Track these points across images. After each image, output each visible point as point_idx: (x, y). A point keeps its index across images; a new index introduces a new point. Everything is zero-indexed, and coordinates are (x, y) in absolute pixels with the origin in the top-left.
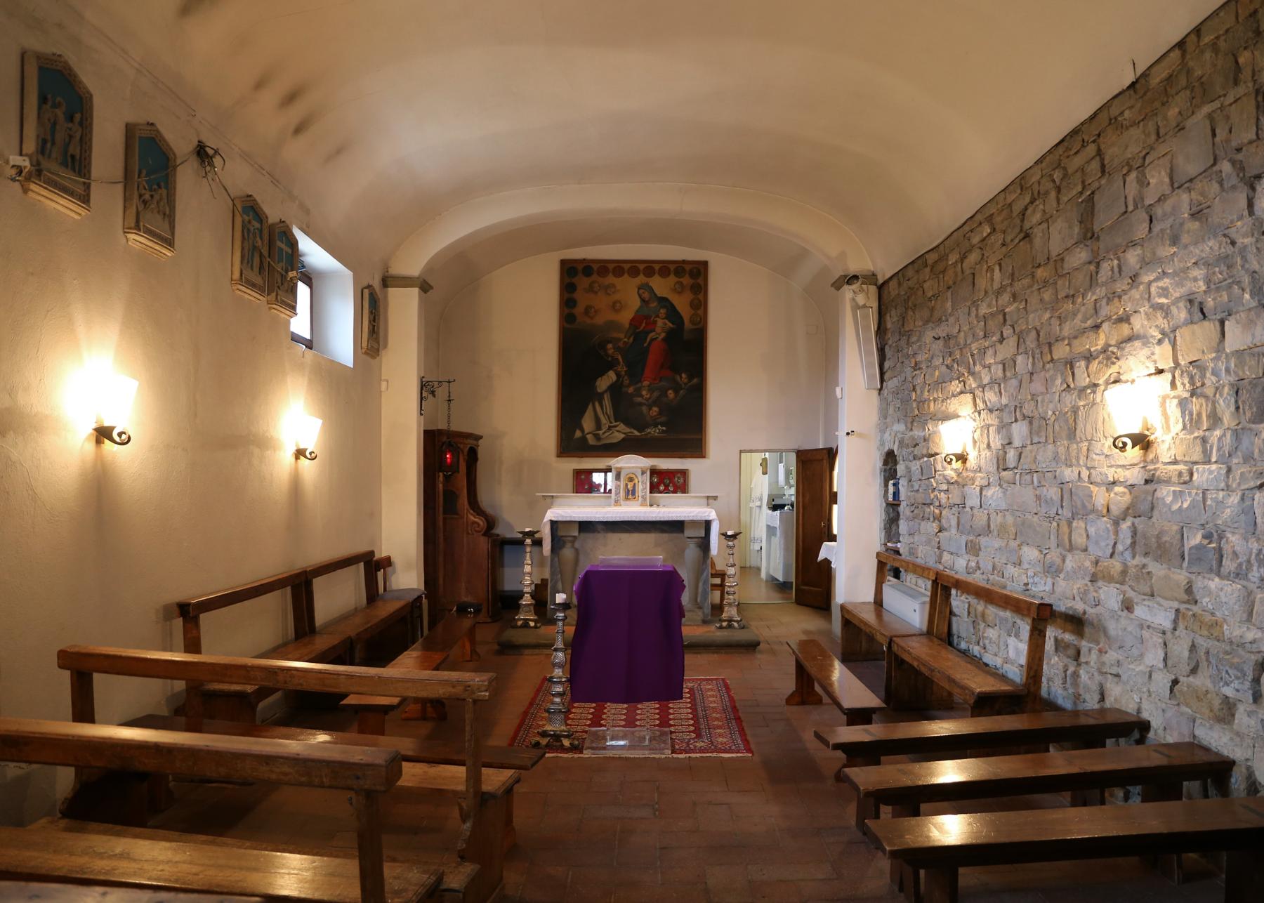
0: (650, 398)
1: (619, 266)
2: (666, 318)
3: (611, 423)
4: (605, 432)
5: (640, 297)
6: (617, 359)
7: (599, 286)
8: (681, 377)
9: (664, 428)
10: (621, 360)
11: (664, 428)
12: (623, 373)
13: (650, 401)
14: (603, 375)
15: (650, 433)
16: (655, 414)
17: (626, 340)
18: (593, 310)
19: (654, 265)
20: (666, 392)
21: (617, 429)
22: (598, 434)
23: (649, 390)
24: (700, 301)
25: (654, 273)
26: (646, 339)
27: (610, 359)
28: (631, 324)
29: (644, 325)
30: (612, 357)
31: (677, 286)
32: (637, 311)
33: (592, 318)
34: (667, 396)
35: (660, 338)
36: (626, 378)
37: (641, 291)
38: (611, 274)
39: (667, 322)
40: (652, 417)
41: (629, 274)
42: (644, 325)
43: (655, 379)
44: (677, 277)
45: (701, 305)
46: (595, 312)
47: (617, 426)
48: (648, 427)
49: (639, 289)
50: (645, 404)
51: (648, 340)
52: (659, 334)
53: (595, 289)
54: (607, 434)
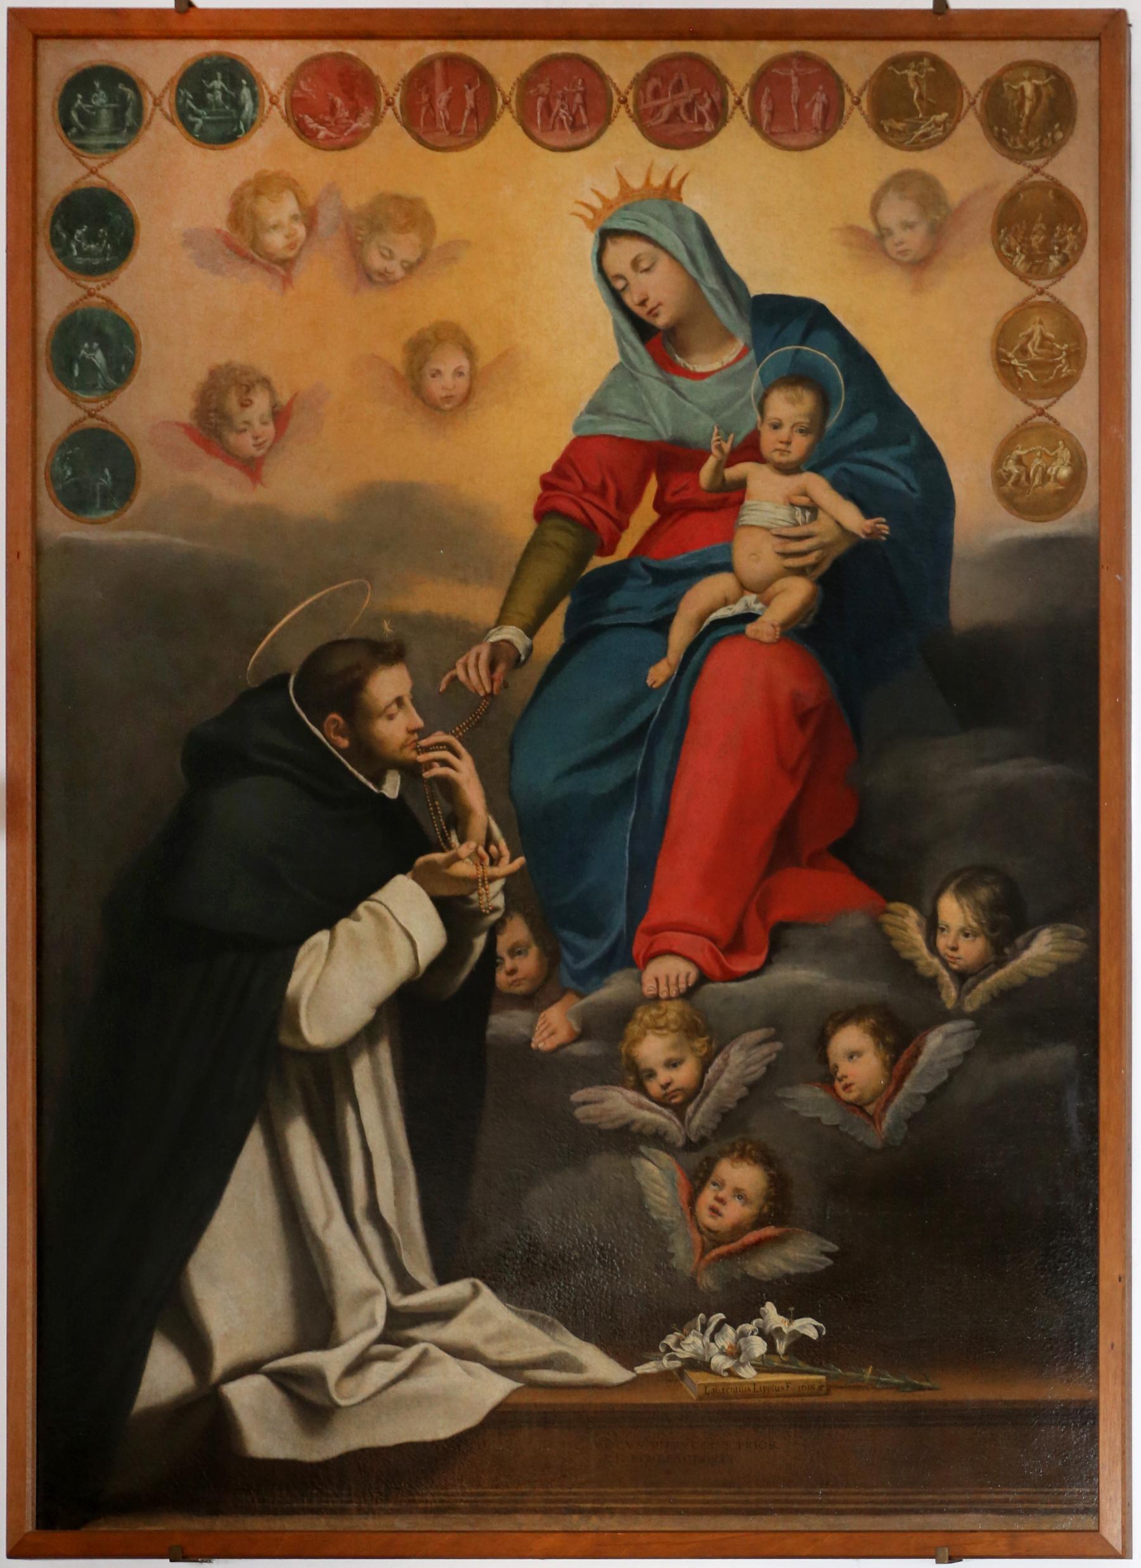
0: (696, 1091)
1: (451, 62)
2: (815, 463)
3: (407, 1285)
4: (359, 1365)
5: (617, 298)
6: (448, 787)
7: (309, 217)
8: (932, 927)
9: (808, 1327)
10: (473, 794)
11: (808, 1327)
12: (494, 897)
13: (701, 1116)
14: (347, 909)
15: (699, 1364)
16: (735, 1212)
17: (511, 633)
18: (261, 403)
19: (712, 50)
20: (822, 1041)
21: (455, 1331)
22: (316, 1377)
23: (691, 1029)
24: (1071, 328)
25: (719, 116)
26: (662, 626)
27: (391, 787)
28: (541, 515)
29: (644, 516)
30: (411, 772)
31: (896, 212)
32: (596, 407)
33: (252, 468)
34: (828, 1078)
35: (765, 628)
36: (517, 931)
37: (620, 255)
38: (391, 125)
39: (818, 487)
40: (714, 1239)
41: (526, 122)
42: (644, 516)
43: (735, 945)
44: (888, 136)
45: (1077, 357)
46: (280, 416)
47: (444, 1314)
48: (681, 1320)
49: (606, 236)
50: (658, 1139)
51: (680, 634)
52: (763, 589)
53: (276, 241)
54: (379, 1373)
